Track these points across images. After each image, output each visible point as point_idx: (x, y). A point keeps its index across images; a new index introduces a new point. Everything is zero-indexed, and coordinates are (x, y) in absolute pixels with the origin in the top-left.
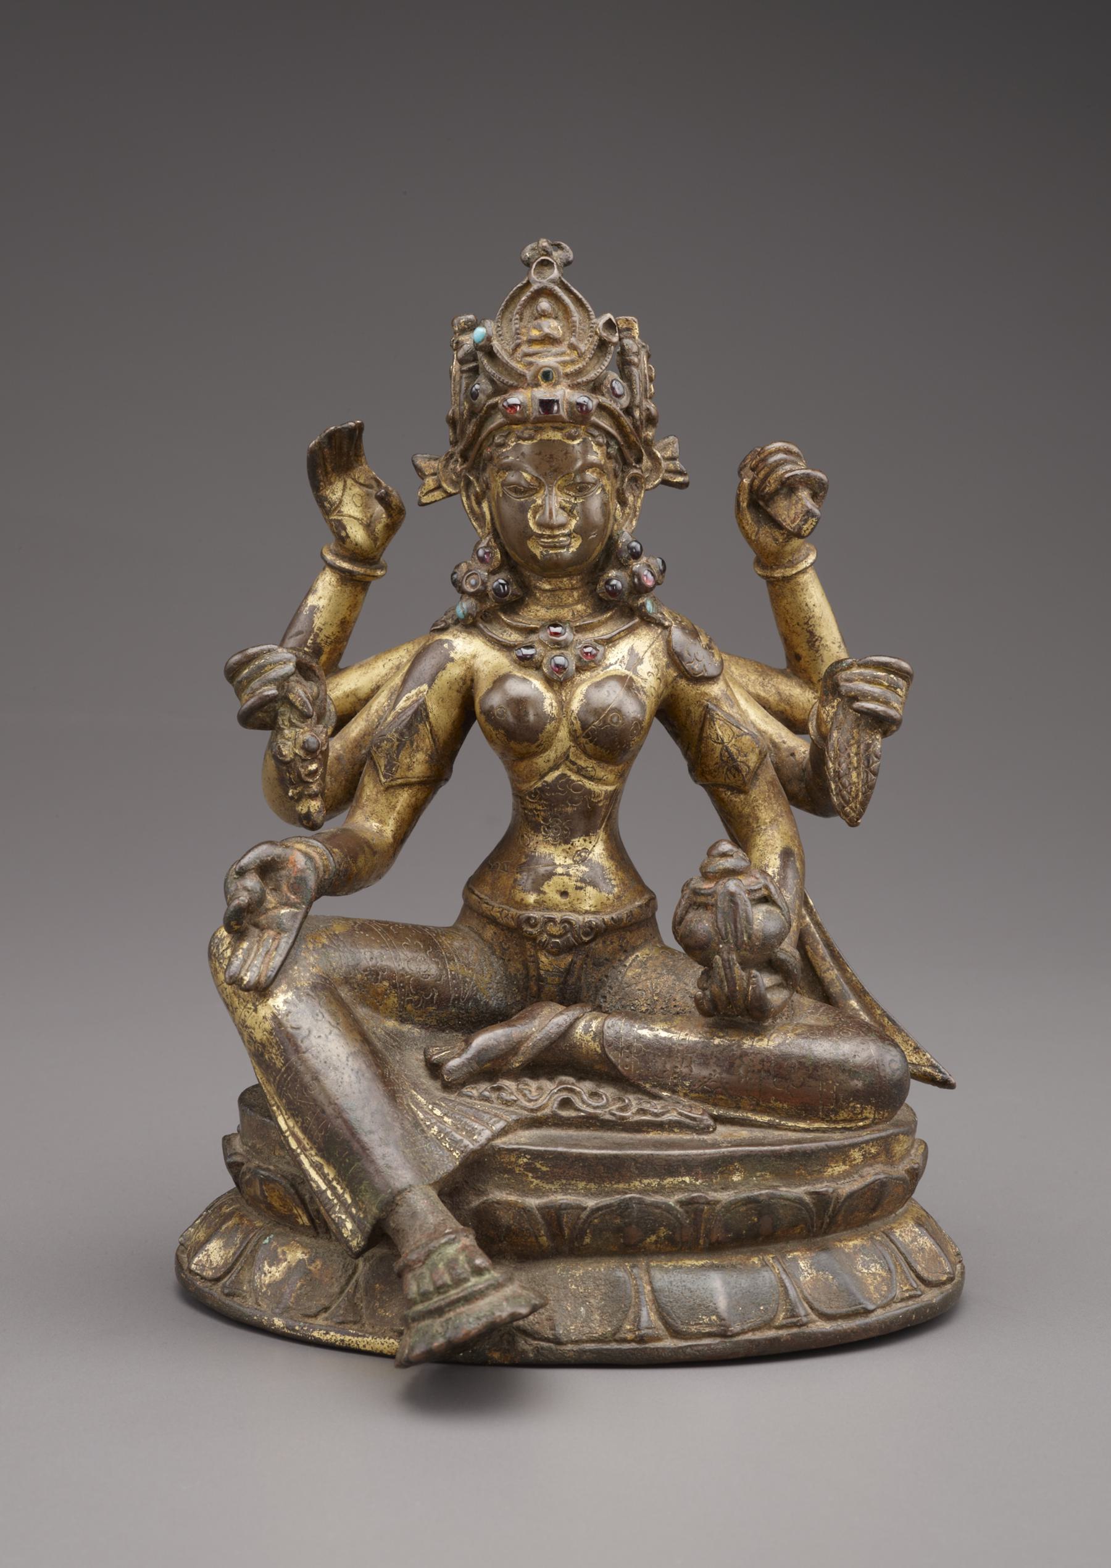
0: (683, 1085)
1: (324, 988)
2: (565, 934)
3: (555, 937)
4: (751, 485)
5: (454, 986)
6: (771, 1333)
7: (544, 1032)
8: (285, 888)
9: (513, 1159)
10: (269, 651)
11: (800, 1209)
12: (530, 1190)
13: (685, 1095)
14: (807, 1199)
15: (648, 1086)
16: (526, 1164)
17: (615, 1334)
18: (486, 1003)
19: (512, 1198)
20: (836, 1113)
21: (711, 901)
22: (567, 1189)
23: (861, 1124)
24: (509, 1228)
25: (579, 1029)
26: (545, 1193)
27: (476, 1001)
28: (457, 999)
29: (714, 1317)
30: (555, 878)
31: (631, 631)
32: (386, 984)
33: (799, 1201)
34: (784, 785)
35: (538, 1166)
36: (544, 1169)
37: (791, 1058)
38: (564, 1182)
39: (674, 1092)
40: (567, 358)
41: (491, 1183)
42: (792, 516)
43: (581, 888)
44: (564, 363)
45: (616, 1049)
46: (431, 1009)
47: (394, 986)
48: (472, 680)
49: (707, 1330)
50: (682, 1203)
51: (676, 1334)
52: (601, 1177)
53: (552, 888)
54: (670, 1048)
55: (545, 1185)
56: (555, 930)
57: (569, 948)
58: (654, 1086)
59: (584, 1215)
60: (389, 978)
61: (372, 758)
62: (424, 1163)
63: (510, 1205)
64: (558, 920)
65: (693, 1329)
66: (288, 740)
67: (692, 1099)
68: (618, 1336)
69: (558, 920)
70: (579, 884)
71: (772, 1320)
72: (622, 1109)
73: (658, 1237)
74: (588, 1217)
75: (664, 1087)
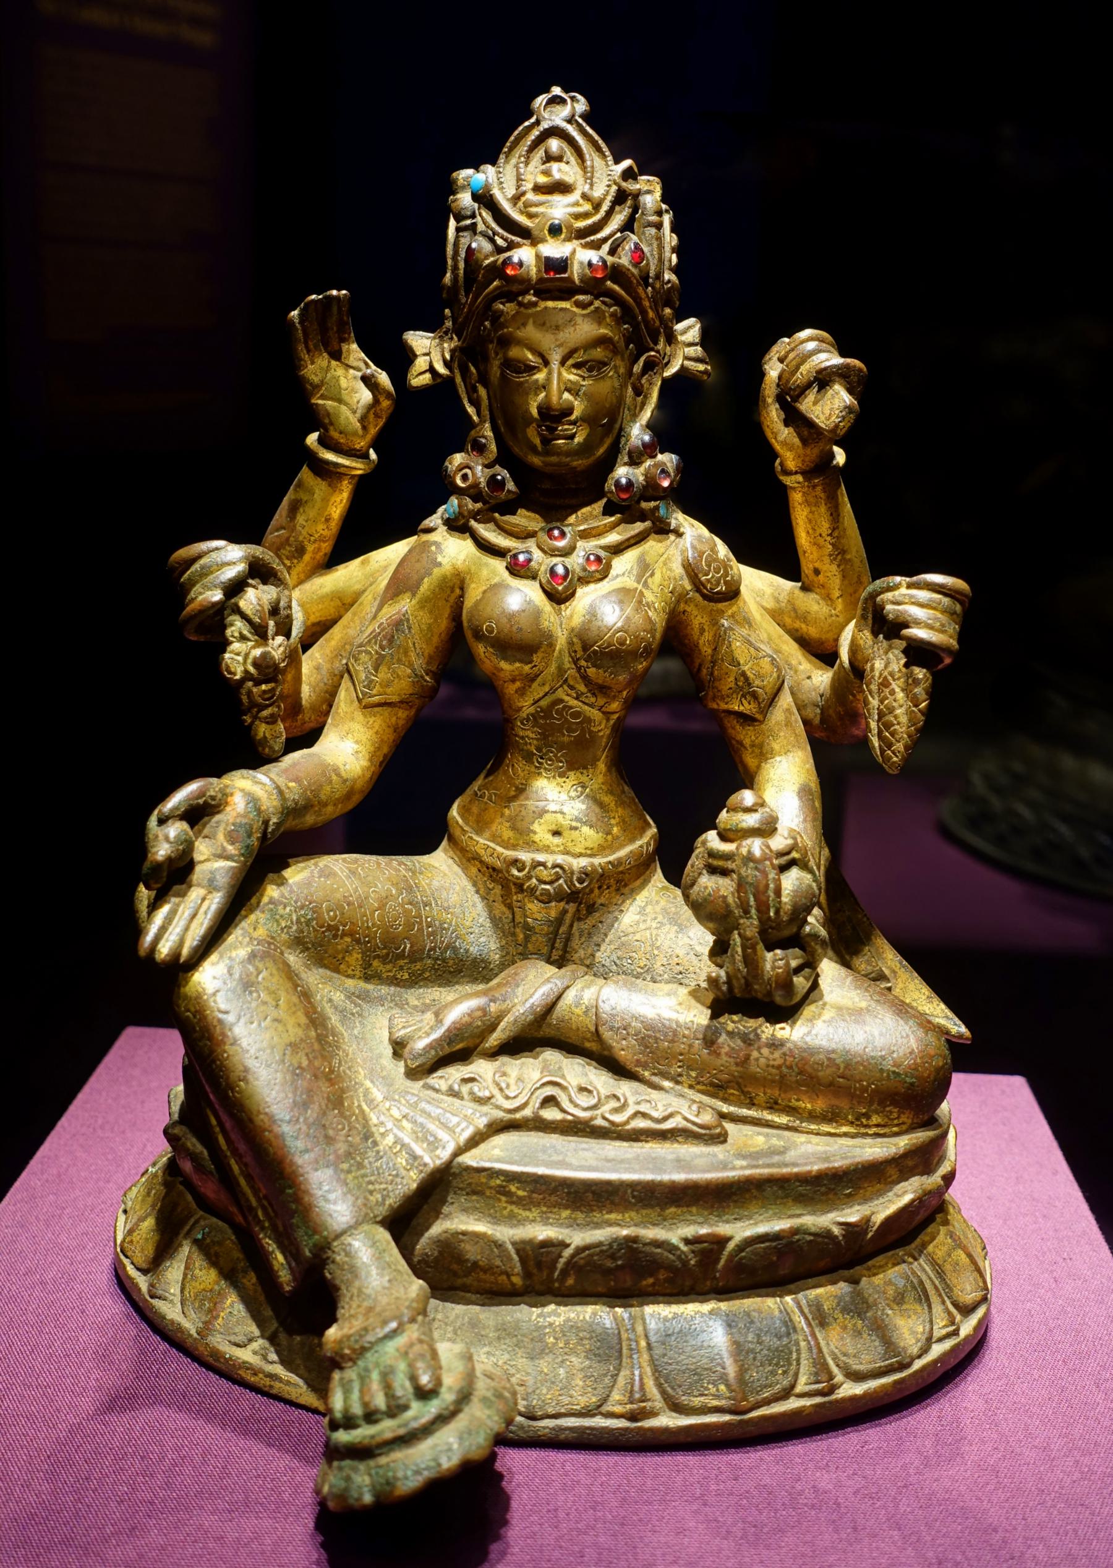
0: (689, 1076)
1: (265, 956)
2: (557, 880)
3: (545, 883)
4: (780, 377)
5: (429, 935)
6: (793, 1404)
7: (528, 1005)
8: (221, 837)
9: (484, 1180)
10: (217, 549)
11: (827, 1244)
12: (502, 1216)
13: (691, 1087)
14: (836, 1231)
15: (646, 1074)
16: (500, 1186)
17: (600, 1406)
18: (467, 951)
19: (480, 1227)
20: (868, 1118)
21: (730, 865)
22: (548, 1218)
23: (895, 1129)
24: (475, 1264)
25: (570, 997)
26: (521, 1222)
27: (455, 950)
28: (433, 949)
29: (722, 1387)
30: (547, 816)
31: (639, 539)
32: (348, 939)
33: (827, 1234)
34: (799, 710)
35: (513, 1189)
36: (521, 1193)
37: (819, 1053)
38: (545, 1209)
39: (677, 1083)
40: (580, 210)
41: (455, 1205)
42: (827, 412)
43: (576, 828)
44: (578, 217)
45: (611, 1029)
46: (401, 962)
47: (358, 941)
48: (462, 589)
49: (715, 1403)
50: (687, 1241)
51: (677, 1408)
52: (590, 1206)
53: (545, 827)
54: (675, 1032)
55: (521, 1212)
56: (545, 874)
57: (560, 896)
58: (654, 1074)
59: (567, 1253)
60: (351, 934)
61: (349, 672)
62: (371, 1192)
63: (477, 1236)
64: (549, 865)
65: (697, 1401)
66: (238, 654)
67: (699, 1091)
68: (606, 1408)
69: (549, 865)
70: (574, 824)
71: (793, 1386)
72: (616, 1110)
73: (657, 1279)
74: (573, 1256)
75: (665, 1075)
